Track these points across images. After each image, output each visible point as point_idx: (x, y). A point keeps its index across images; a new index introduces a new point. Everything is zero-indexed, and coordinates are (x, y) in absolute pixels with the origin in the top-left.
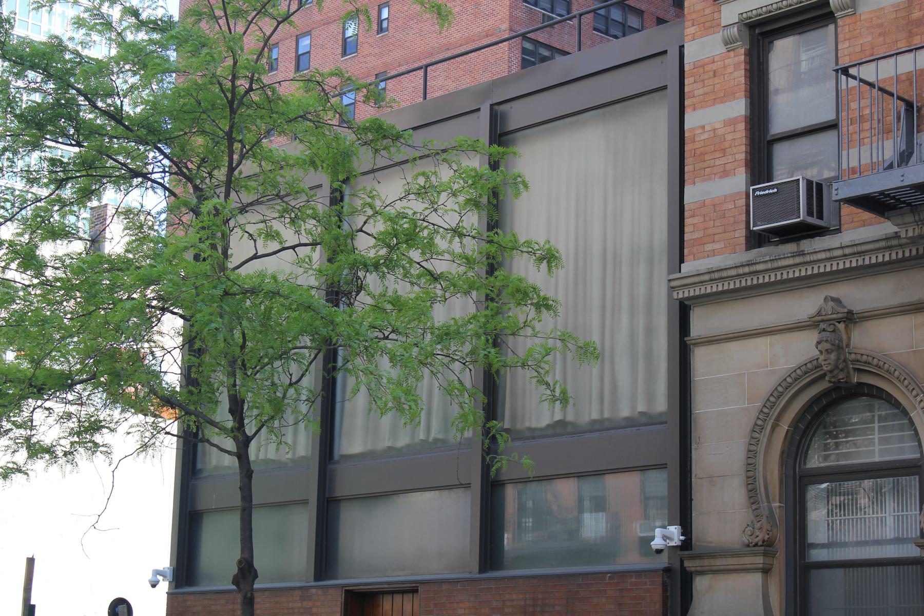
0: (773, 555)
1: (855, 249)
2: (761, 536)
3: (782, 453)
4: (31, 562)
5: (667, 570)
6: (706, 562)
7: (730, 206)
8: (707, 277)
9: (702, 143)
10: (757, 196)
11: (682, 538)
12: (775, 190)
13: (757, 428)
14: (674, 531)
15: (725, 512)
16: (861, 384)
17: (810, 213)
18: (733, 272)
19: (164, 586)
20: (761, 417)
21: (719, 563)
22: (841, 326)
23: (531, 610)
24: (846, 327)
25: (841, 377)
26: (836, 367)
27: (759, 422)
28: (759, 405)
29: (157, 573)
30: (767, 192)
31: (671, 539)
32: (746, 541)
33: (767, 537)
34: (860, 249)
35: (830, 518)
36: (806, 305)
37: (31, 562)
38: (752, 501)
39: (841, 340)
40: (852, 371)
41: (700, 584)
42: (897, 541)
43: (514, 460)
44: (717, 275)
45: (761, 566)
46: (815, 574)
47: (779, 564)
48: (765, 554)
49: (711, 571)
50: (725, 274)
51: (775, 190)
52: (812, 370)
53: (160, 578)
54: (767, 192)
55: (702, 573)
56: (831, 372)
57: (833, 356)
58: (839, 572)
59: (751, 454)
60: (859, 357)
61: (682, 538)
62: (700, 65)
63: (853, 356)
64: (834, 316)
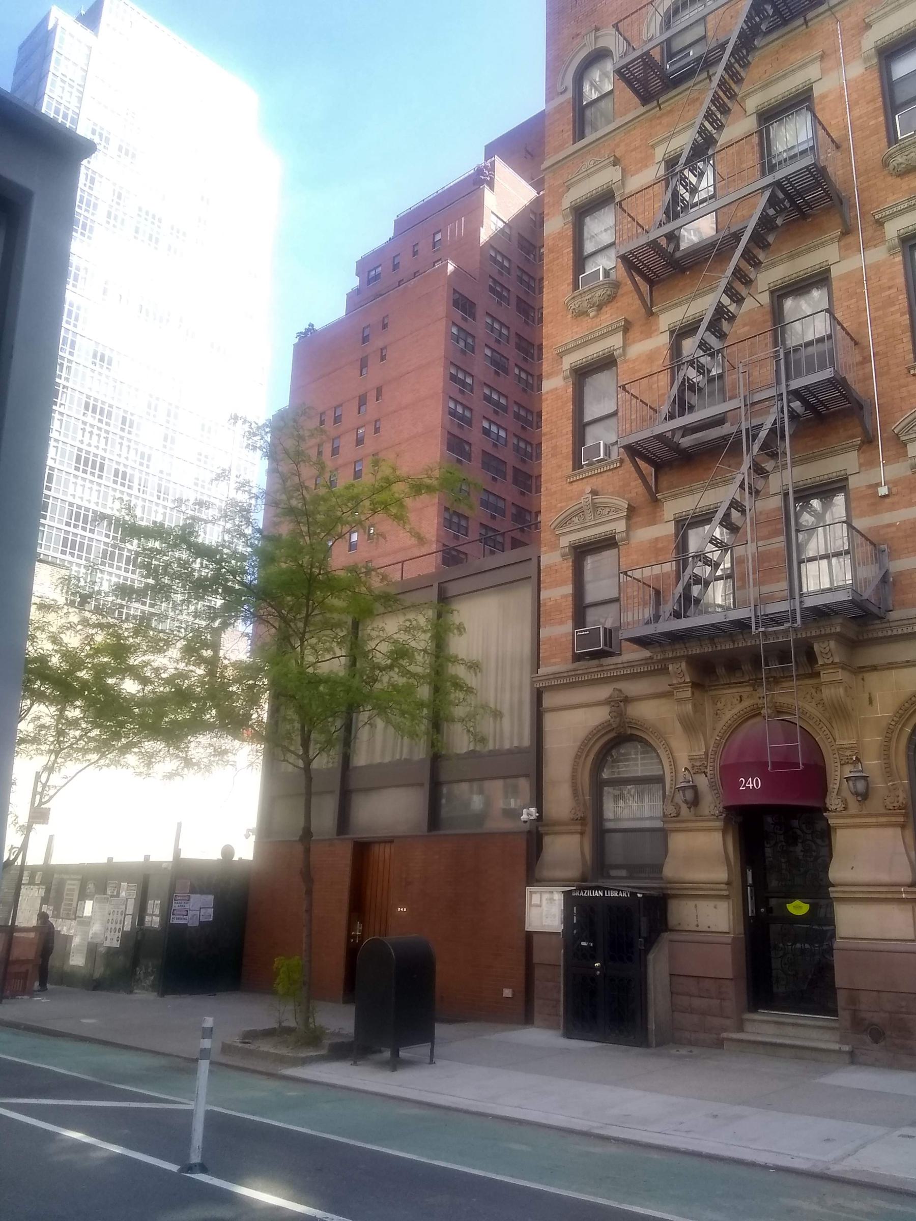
1: (629, 664)
2: (580, 815)
4: (179, 825)
5: (529, 832)
7: (564, 639)
13: (577, 757)
14: (533, 810)
15: (561, 800)
16: (632, 735)
17: (605, 645)
18: (565, 674)
19: (253, 838)
21: (557, 828)
22: (622, 704)
28: (579, 744)
29: (249, 830)
36: (604, 692)
37: (179, 825)
41: (547, 840)
42: (651, 818)
44: (557, 676)
46: (607, 835)
47: (589, 829)
48: (582, 825)
50: (561, 675)
55: (547, 834)
59: (574, 770)
62: (549, 567)
63: (628, 720)
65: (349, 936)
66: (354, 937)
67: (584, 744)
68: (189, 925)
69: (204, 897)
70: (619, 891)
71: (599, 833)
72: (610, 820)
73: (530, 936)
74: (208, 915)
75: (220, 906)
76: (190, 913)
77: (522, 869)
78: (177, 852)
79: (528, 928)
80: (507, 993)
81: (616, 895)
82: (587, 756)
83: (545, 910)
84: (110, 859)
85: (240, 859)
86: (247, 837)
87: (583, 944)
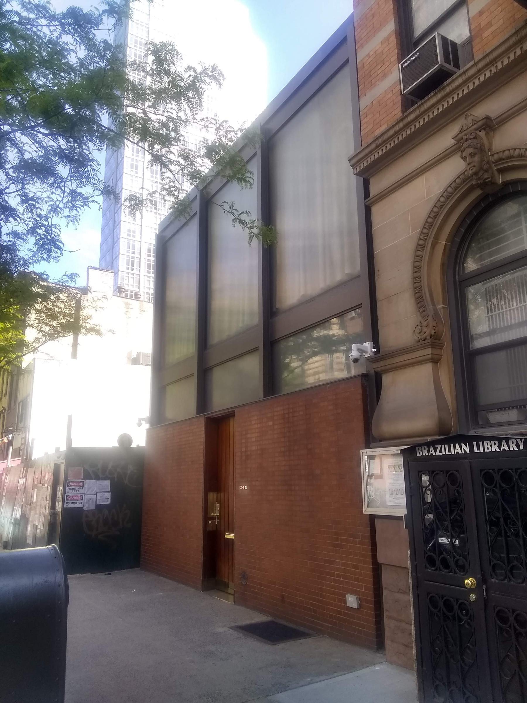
0: (441, 347)
1: (487, 60)
2: (429, 331)
3: (443, 264)
4: (70, 418)
5: (365, 376)
6: (388, 362)
8: (373, 146)
9: (369, 65)
10: (405, 67)
11: (374, 350)
12: (418, 54)
13: (420, 247)
14: (368, 346)
15: (402, 321)
16: (506, 184)
17: (446, 58)
18: (391, 132)
20: (422, 237)
21: (398, 360)
22: (482, 134)
23: (287, 416)
24: (487, 134)
25: (486, 176)
26: (481, 168)
27: (421, 242)
30: (412, 59)
31: (366, 352)
32: (417, 339)
33: (433, 333)
34: (491, 57)
35: (490, 314)
37: (70, 418)
38: (419, 305)
39: (482, 145)
40: (496, 173)
41: (386, 379)
43: (283, 326)
44: (380, 141)
45: (430, 356)
46: (479, 359)
47: (447, 354)
48: (433, 346)
49: (392, 368)
50: (386, 137)
51: (418, 54)
52: (460, 185)
53: (142, 421)
54: (412, 59)
55: (386, 371)
56: (476, 174)
57: (477, 159)
58: (502, 355)
59: (417, 269)
60: (501, 155)
61: (374, 350)
63: (496, 156)
64: (475, 126)
65: (207, 517)
66: (213, 518)
67: (428, 225)
68: (85, 508)
69: (99, 482)
70: (500, 440)
71: (468, 361)
72: (481, 336)
73: (373, 518)
74: (106, 498)
75: (118, 490)
76: (86, 498)
77: (358, 425)
78: (69, 441)
79: (369, 511)
80: (352, 601)
81: (495, 448)
82: (433, 246)
83: (384, 482)
84: (46, 454)
85: (138, 446)
86: (139, 425)
87: (443, 540)
